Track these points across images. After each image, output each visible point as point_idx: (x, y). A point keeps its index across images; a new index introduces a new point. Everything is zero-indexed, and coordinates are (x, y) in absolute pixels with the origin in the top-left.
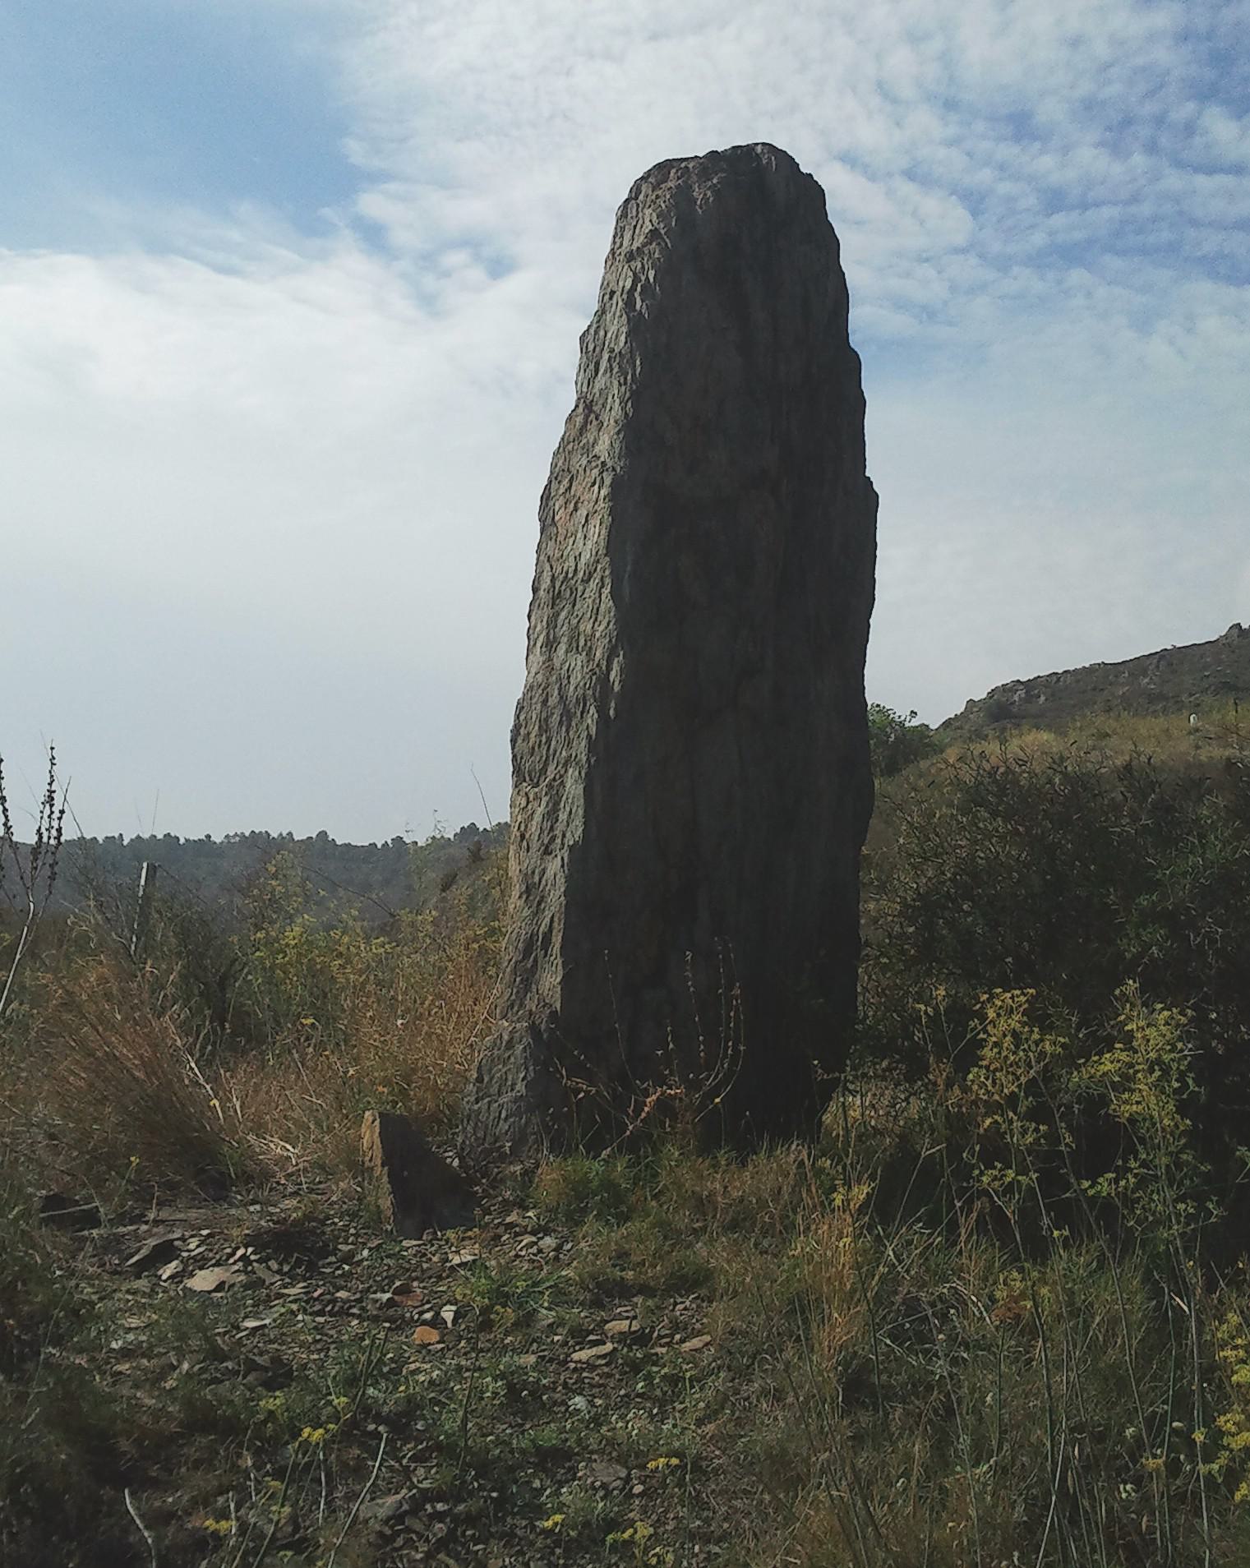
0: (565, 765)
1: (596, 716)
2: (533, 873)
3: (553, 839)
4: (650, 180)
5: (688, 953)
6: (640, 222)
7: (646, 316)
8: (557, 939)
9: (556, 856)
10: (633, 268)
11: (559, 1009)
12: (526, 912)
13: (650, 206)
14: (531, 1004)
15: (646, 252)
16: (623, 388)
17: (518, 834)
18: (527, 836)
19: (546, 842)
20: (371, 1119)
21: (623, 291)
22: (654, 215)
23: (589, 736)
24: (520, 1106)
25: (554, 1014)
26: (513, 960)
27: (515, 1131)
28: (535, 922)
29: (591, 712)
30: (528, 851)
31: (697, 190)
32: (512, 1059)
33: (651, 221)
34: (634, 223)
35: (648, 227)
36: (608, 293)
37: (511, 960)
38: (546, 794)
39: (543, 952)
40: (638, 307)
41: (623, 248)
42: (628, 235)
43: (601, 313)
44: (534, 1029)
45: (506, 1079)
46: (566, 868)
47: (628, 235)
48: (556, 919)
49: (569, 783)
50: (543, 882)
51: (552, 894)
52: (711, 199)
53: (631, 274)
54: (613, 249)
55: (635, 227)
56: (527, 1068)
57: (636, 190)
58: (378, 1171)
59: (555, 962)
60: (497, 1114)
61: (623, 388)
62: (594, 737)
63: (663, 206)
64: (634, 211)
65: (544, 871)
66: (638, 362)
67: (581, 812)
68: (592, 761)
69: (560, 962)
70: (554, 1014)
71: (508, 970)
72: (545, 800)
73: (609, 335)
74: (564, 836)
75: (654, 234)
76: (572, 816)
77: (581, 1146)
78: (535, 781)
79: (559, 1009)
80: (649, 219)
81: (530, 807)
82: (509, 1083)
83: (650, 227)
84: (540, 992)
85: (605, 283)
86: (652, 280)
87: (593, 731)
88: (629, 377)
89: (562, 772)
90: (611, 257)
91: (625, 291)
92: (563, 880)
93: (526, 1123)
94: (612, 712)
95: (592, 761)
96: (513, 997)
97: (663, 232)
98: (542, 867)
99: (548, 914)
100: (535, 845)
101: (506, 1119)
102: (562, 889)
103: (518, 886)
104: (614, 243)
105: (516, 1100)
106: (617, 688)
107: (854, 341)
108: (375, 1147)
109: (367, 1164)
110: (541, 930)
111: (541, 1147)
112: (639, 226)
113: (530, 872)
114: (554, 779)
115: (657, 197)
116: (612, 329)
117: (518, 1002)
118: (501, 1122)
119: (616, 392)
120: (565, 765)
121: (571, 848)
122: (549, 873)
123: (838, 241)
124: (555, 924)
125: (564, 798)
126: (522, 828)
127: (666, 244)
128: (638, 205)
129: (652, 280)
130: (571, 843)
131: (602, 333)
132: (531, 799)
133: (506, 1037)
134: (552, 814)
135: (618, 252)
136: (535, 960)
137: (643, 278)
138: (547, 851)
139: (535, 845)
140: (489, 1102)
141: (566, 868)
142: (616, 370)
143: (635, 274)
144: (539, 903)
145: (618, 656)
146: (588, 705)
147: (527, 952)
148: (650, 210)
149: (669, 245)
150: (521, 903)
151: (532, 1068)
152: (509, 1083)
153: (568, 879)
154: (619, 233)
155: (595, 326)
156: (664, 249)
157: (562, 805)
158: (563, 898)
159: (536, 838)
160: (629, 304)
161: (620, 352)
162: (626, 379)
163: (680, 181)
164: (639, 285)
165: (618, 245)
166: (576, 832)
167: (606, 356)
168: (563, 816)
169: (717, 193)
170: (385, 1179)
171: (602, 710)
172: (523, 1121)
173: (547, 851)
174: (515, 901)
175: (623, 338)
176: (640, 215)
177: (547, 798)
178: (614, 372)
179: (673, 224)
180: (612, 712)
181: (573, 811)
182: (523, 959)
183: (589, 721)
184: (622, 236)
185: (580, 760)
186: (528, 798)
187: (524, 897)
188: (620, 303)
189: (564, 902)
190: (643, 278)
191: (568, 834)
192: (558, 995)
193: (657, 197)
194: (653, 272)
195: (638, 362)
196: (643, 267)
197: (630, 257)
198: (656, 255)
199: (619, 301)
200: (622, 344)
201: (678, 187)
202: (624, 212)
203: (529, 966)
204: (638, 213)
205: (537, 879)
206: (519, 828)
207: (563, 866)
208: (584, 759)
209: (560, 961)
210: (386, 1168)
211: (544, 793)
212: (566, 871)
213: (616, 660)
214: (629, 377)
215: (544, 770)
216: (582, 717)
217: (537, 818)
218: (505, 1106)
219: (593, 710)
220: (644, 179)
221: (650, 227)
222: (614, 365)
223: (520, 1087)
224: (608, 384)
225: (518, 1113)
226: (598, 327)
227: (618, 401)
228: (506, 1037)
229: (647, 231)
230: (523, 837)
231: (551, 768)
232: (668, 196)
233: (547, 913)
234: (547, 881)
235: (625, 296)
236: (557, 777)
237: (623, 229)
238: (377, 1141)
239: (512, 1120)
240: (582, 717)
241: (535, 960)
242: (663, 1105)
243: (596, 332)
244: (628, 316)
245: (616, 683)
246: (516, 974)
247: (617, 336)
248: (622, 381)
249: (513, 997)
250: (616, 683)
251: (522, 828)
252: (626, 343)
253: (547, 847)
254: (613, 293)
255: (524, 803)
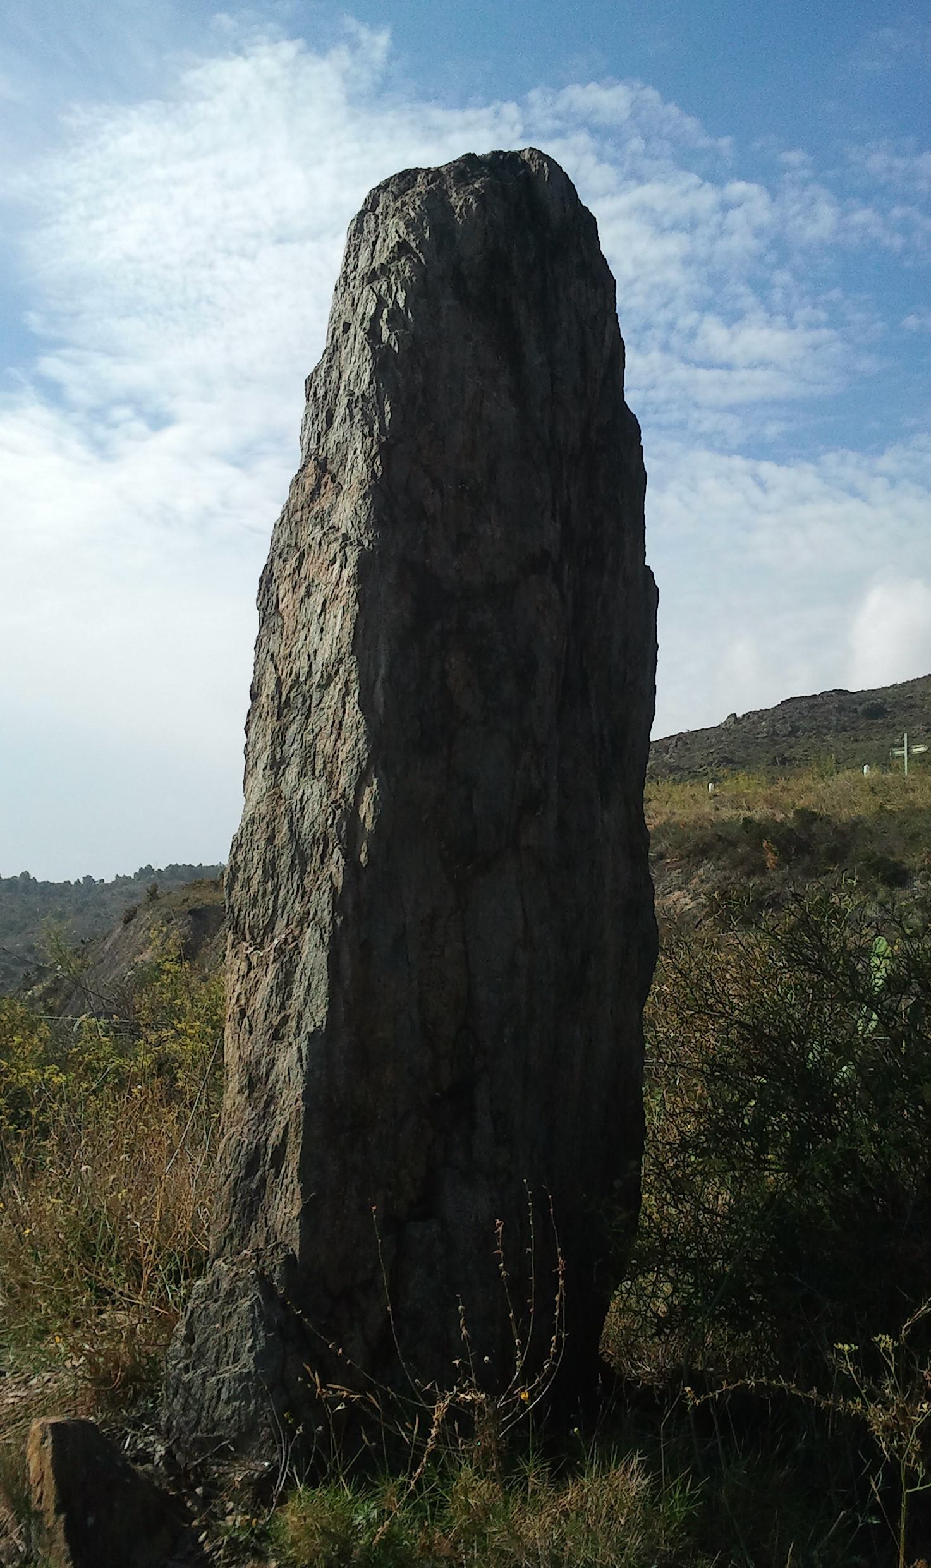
0: (300, 923)
1: (342, 862)
2: (258, 1063)
3: (285, 1020)
4: (389, 189)
5: (498, 1222)
6: (382, 235)
7: (396, 349)
8: (293, 1157)
9: (290, 1044)
10: (376, 291)
11: (297, 1253)
12: (249, 1114)
13: (394, 215)
14: (258, 1239)
15: (393, 269)
16: (369, 440)
17: (237, 1009)
18: (249, 1013)
19: (275, 1023)
20: (39, 1434)
21: (363, 318)
22: (401, 223)
23: (333, 889)
24: (246, 1387)
25: (290, 1260)
26: (232, 1177)
27: (240, 1421)
28: (261, 1128)
29: (335, 856)
30: (251, 1033)
31: (455, 195)
32: (235, 1317)
33: (397, 232)
34: (374, 239)
35: (393, 240)
36: (340, 328)
37: (228, 1176)
38: (275, 961)
39: (272, 1171)
40: (385, 338)
41: (359, 270)
42: (364, 255)
43: (333, 350)
44: (262, 1279)
45: (226, 1346)
46: (304, 1062)
47: (364, 255)
48: (292, 1130)
49: (305, 949)
50: (272, 1077)
51: (284, 1096)
52: (474, 206)
53: (374, 296)
54: (345, 272)
55: (374, 243)
56: (255, 1334)
57: (372, 201)
58: (50, 1519)
59: (291, 1187)
60: (215, 1393)
61: (369, 440)
62: (340, 888)
63: (413, 214)
64: (372, 224)
65: (272, 1063)
66: (387, 408)
67: (323, 988)
68: (338, 922)
69: (298, 1190)
70: (290, 1260)
71: (226, 1188)
72: (273, 968)
73: (345, 376)
74: (300, 1017)
75: (402, 248)
76: (311, 993)
77: (341, 1478)
78: (259, 940)
79: (297, 1253)
80: (394, 230)
81: (252, 974)
82: (231, 1350)
83: (397, 239)
84: (270, 1224)
85: (336, 315)
86: (401, 305)
87: (339, 881)
88: (376, 426)
89: (297, 933)
90: (342, 282)
91: (367, 319)
92: (300, 1078)
93: (256, 1411)
94: (363, 858)
95: (338, 922)
96: (233, 1226)
97: (413, 245)
98: (271, 1056)
99: (281, 1120)
100: (260, 1026)
101: (228, 1402)
102: (301, 1091)
103: (237, 1076)
104: (347, 265)
105: (241, 1378)
106: (369, 825)
107: (632, 399)
108: (45, 1482)
109: (34, 1506)
110: (270, 1142)
111: (278, 1446)
112: (380, 240)
113: (253, 1062)
114: (286, 941)
115: (404, 204)
116: (349, 370)
117: (239, 1233)
118: (221, 1404)
119: (359, 446)
120: (300, 923)
121: (312, 1036)
122: (281, 1067)
123: (615, 281)
124: (291, 1136)
125: (300, 967)
126: (242, 1002)
127: (419, 260)
128: (377, 217)
129: (401, 305)
130: (311, 1029)
131: (335, 374)
132: (254, 963)
133: (225, 1285)
134: (283, 987)
135: (352, 276)
136: (263, 1180)
137: (390, 302)
138: (277, 1036)
139: (260, 1026)
140: (204, 1376)
141: (304, 1062)
142: (358, 417)
143: (379, 297)
144: (267, 1104)
145: (371, 785)
146: (331, 846)
147: (252, 1166)
148: (396, 220)
149: (423, 261)
150: (241, 1099)
151: (262, 1334)
152: (231, 1350)
153: (308, 1076)
154: (353, 252)
155: (325, 366)
156: (417, 267)
157: (297, 976)
158: (300, 1103)
159: (262, 1018)
160: (373, 333)
161: (363, 395)
162: (371, 429)
163: (432, 186)
164: (385, 311)
165: (351, 267)
166: (317, 1014)
167: (344, 401)
168: (298, 991)
169: (480, 198)
170: (60, 1535)
171: (350, 854)
172: (252, 1407)
173: (277, 1036)
174: (232, 1095)
175: (366, 377)
176: (381, 227)
177: (277, 966)
178: (356, 421)
179: (427, 235)
180: (363, 858)
181: (313, 986)
182: (247, 1175)
183: (333, 868)
184: (357, 257)
185: (321, 919)
186: (250, 964)
187: (246, 1093)
188: (361, 334)
189: (303, 1108)
190: (390, 302)
191: (307, 1015)
192: (296, 1234)
193: (404, 204)
194: (404, 294)
195: (387, 408)
196: (390, 288)
197: (372, 277)
198: (407, 274)
199: (359, 334)
200: (365, 385)
201: (429, 192)
202: (358, 229)
203: (254, 1186)
204: (377, 226)
205: (263, 1070)
206: (238, 1000)
207: (300, 1059)
208: (328, 919)
209: (297, 1186)
210: (62, 1517)
211: (272, 958)
212: (305, 1067)
213: (368, 790)
214: (376, 426)
215: (270, 927)
216: (322, 862)
217: (263, 991)
218: (226, 1384)
219: (337, 854)
220: (383, 187)
221: (397, 239)
222: (355, 411)
223: (247, 1360)
224: (348, 435)
225: (245, 1396)
226: (331, 367)
227: (361, 456)
228: (225, 1285)
229: (392, 245)
230: (243, 1013)
231: (280, 925)
232: (418, 203)
233: (278, 1118)
234: (278, 1075)
235: (366, 324)
236: (290, 940)
237: (357, 248)
238: (49, 1472)
239: (237, 1404)
240: (322, 862)
241: (263, 1180)
242: (457, 1412)
243: (328, 373)
244: (372, 348)
245: (369, 820)
246: (235, 1196)
247: (358, 375)
248: (366, 430)
249: (233, 1226)
250: (369, 820)
251: (242, 1002)
252: (371, 383)
253: (277, 1030)
254: (347, 326)
255: (244, 968)
